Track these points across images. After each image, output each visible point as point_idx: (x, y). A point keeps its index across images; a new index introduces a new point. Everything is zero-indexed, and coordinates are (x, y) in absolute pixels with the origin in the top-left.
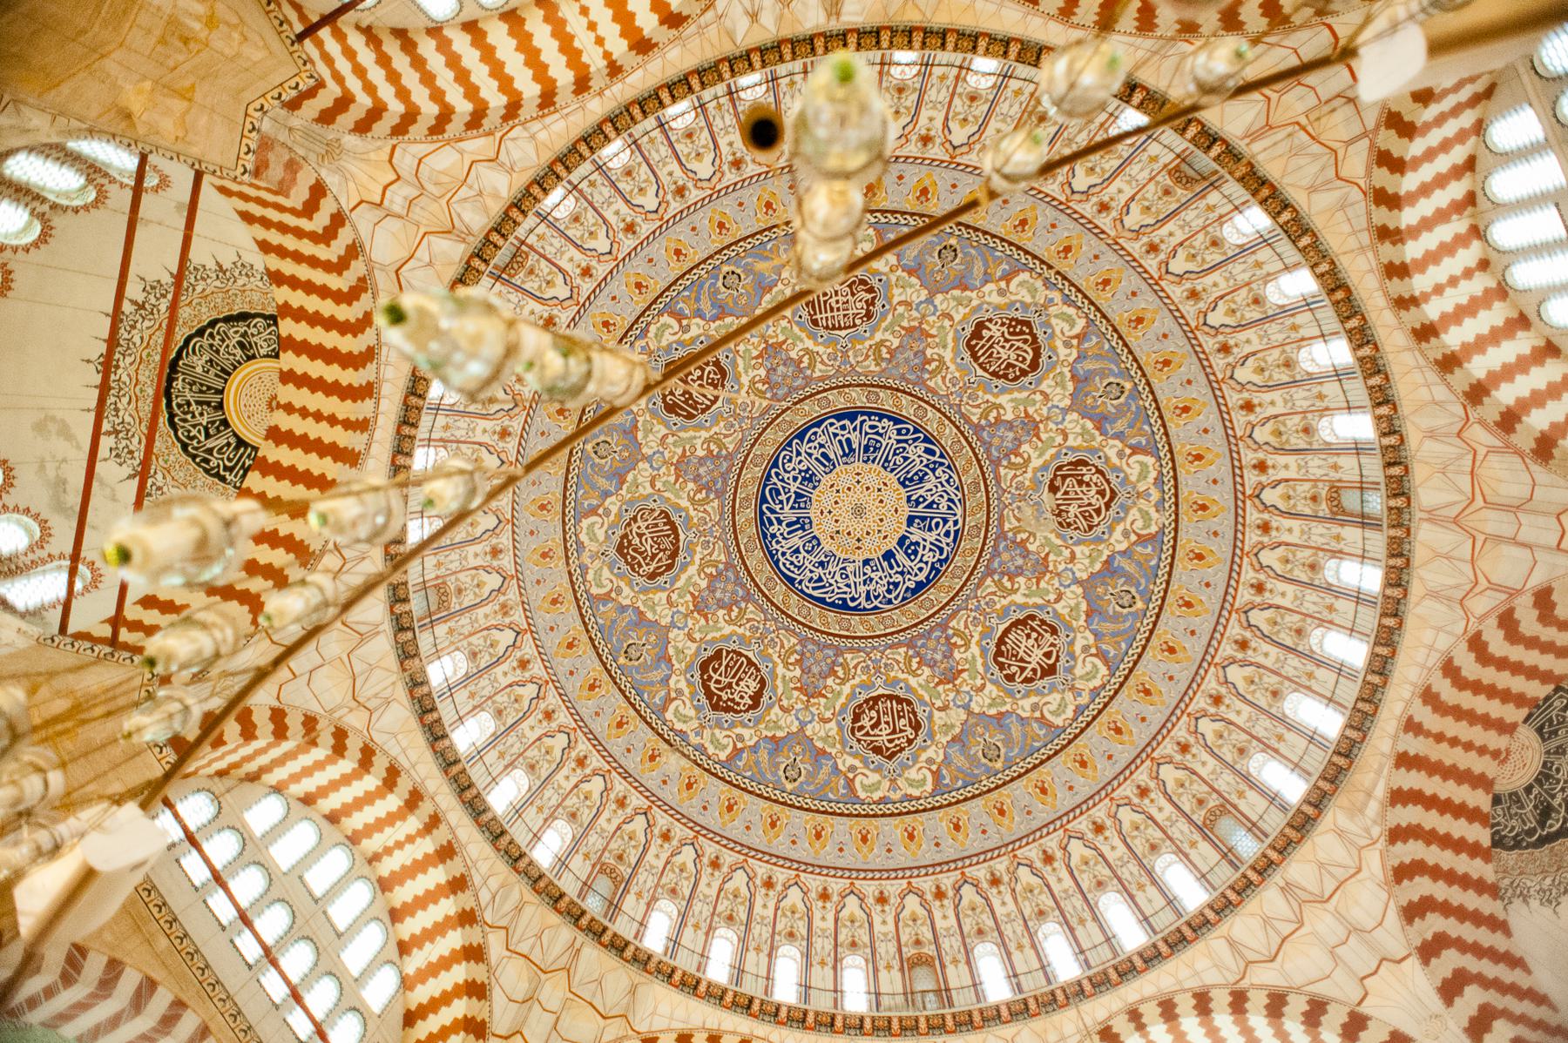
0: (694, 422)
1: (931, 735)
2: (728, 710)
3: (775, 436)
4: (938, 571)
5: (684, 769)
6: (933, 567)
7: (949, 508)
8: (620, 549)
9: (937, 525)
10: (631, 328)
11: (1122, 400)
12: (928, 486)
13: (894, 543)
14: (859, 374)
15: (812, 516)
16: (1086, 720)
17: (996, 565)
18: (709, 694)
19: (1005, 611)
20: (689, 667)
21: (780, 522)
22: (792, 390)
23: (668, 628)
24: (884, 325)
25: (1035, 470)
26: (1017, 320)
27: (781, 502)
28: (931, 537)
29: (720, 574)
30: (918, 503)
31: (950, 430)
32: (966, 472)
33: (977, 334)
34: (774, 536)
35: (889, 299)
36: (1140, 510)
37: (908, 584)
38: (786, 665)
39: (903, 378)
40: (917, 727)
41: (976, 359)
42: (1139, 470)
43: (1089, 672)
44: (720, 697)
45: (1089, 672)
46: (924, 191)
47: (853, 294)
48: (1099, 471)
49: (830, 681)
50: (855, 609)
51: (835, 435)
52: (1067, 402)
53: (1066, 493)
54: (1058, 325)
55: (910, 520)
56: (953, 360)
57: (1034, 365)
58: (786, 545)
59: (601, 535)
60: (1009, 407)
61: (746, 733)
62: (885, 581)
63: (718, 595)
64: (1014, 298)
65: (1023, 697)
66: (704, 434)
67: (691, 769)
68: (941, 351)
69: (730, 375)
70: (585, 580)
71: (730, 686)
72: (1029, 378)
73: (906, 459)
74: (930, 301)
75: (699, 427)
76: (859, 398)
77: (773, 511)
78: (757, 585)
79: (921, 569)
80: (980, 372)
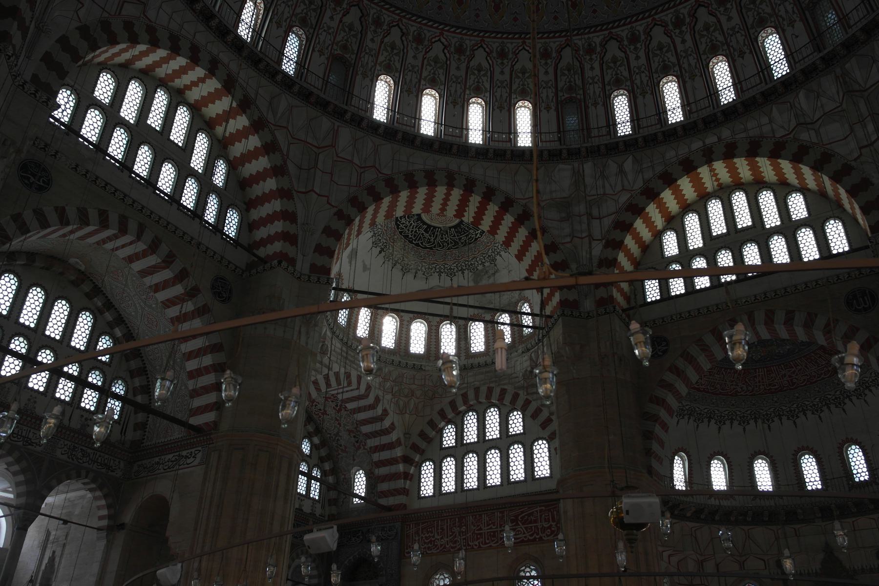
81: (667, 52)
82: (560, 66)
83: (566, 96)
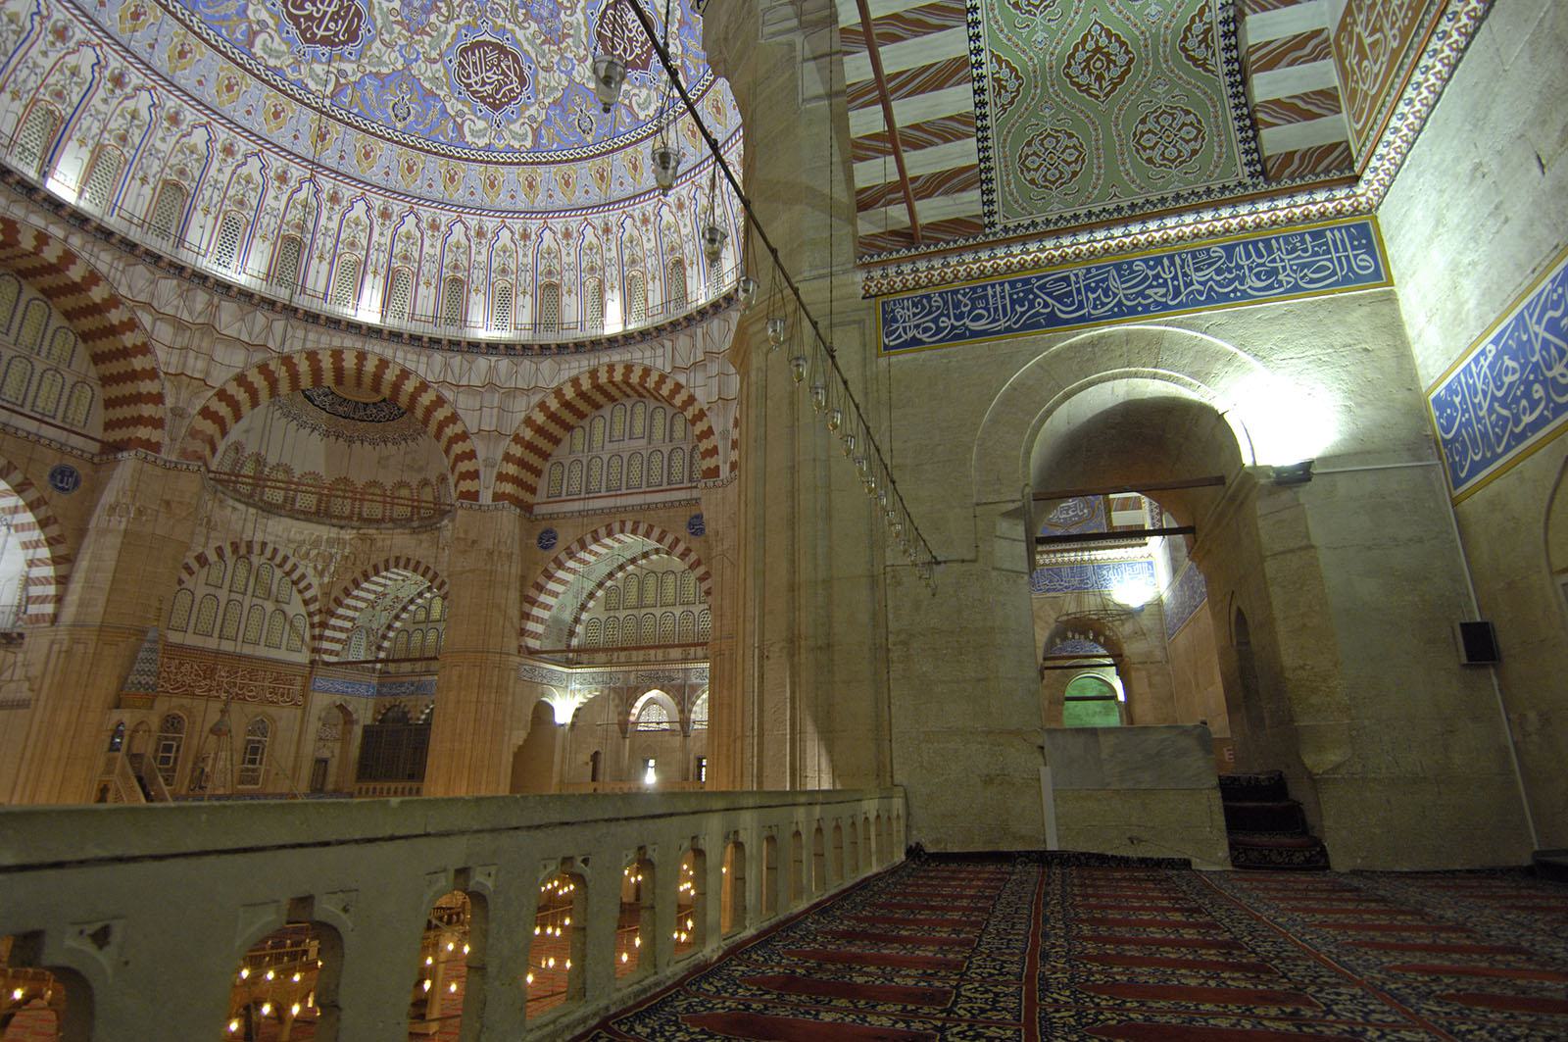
0: (364, 9)
10: (276, 87)
23: (571, 81)
59: (481, 124)
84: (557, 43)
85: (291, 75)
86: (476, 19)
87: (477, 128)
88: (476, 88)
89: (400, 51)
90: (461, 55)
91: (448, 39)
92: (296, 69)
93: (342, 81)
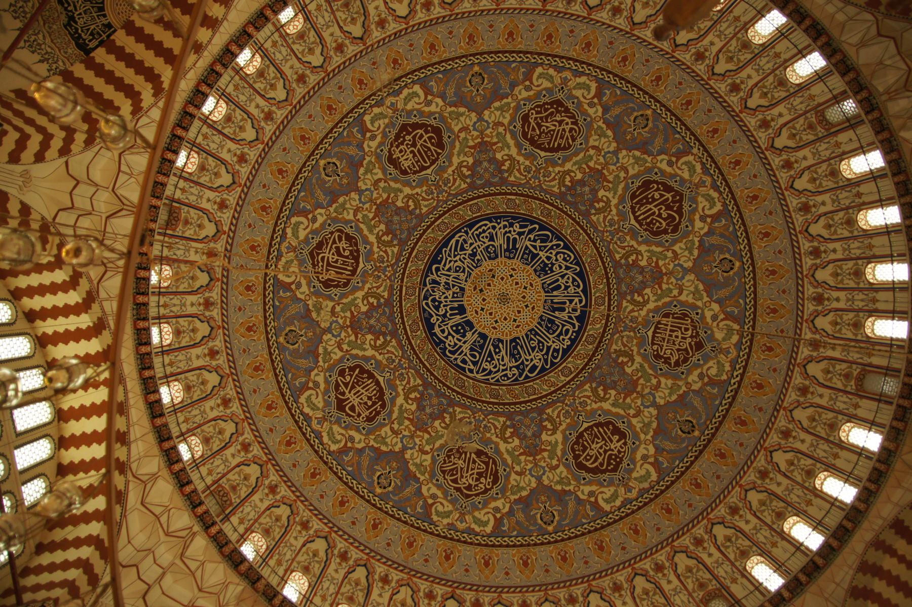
1: (317, 294)
2: (397, 137)
3: (588, 254)
4: (437, 344)
5: (374, 82)
6: (441, 341)
7: (484, 370)
8: (559, 103)
9: (474, 356)
10: (724, 179)
11: (540, 521)
12: (506, 359)
13: (470, 318)
14: (613, 335)
15: (515, 261)
16: (301, 421)
17: (430, 391)
18: (416, 126)
19: (393, 387)
20: (443, 119)
21: (520, 234)
22: (620, 281)
24: (646, 365)
25: (497, 444)
26: (620, 462)
27: (535, 241)
28: (466, 348)
29: (501, 172)
30: (496, 347)
31: (546, 389)
32: (509, 392)
33: (616, 431)
34: (511, 225)
35: (665, 375)
36: (451, 512)
37: (435, 317)
38: (409, 197)
39: (598, 367)
40: (327, 284)
41: (597, 425)
42: (484, 519)
43: (335, 435)
44: (409, 133)
45: (335, 435)
46: (743, 423)
47: (678, 350)
48: (486, 491)
49: (383, 227)
50: (430, 268)
51: (571, 301)
52: (546, 482)
53: (474, 462)
54: (608, 492)
55: (483, 336)
56: (601, 408)
57: (581, 466)
58: (500, 232)
59: (578, 93)
60: (552, 439)
61: (374, 144)
62: (442, 300)
63: (485, 164)
64: (638, 465)
65: (326, 378)
66: (614, 202)
67: (371, 89)
68: (610, 401)
69: (652, 238)
70: (550, 66)
71: (414, 145)
72: (571, 459)
73: (533, 349)
74: (654, 404)
75: (622, 200)
76: (594, 328)
77: (530, 232)
78: (479, 197)
79: (443, 331)
80: (586, 425)
81: (841, 269)
82: (821, 381)
83: (853, 383)
84: (483, 143)
85: (708, 180)
86: (545, 169)
87: (583, 90)
88: (567, 120)
89: (618, 161)
90: (570, 146)
91: (575, 159)
92: (702, 183)
93: (674, 159)
